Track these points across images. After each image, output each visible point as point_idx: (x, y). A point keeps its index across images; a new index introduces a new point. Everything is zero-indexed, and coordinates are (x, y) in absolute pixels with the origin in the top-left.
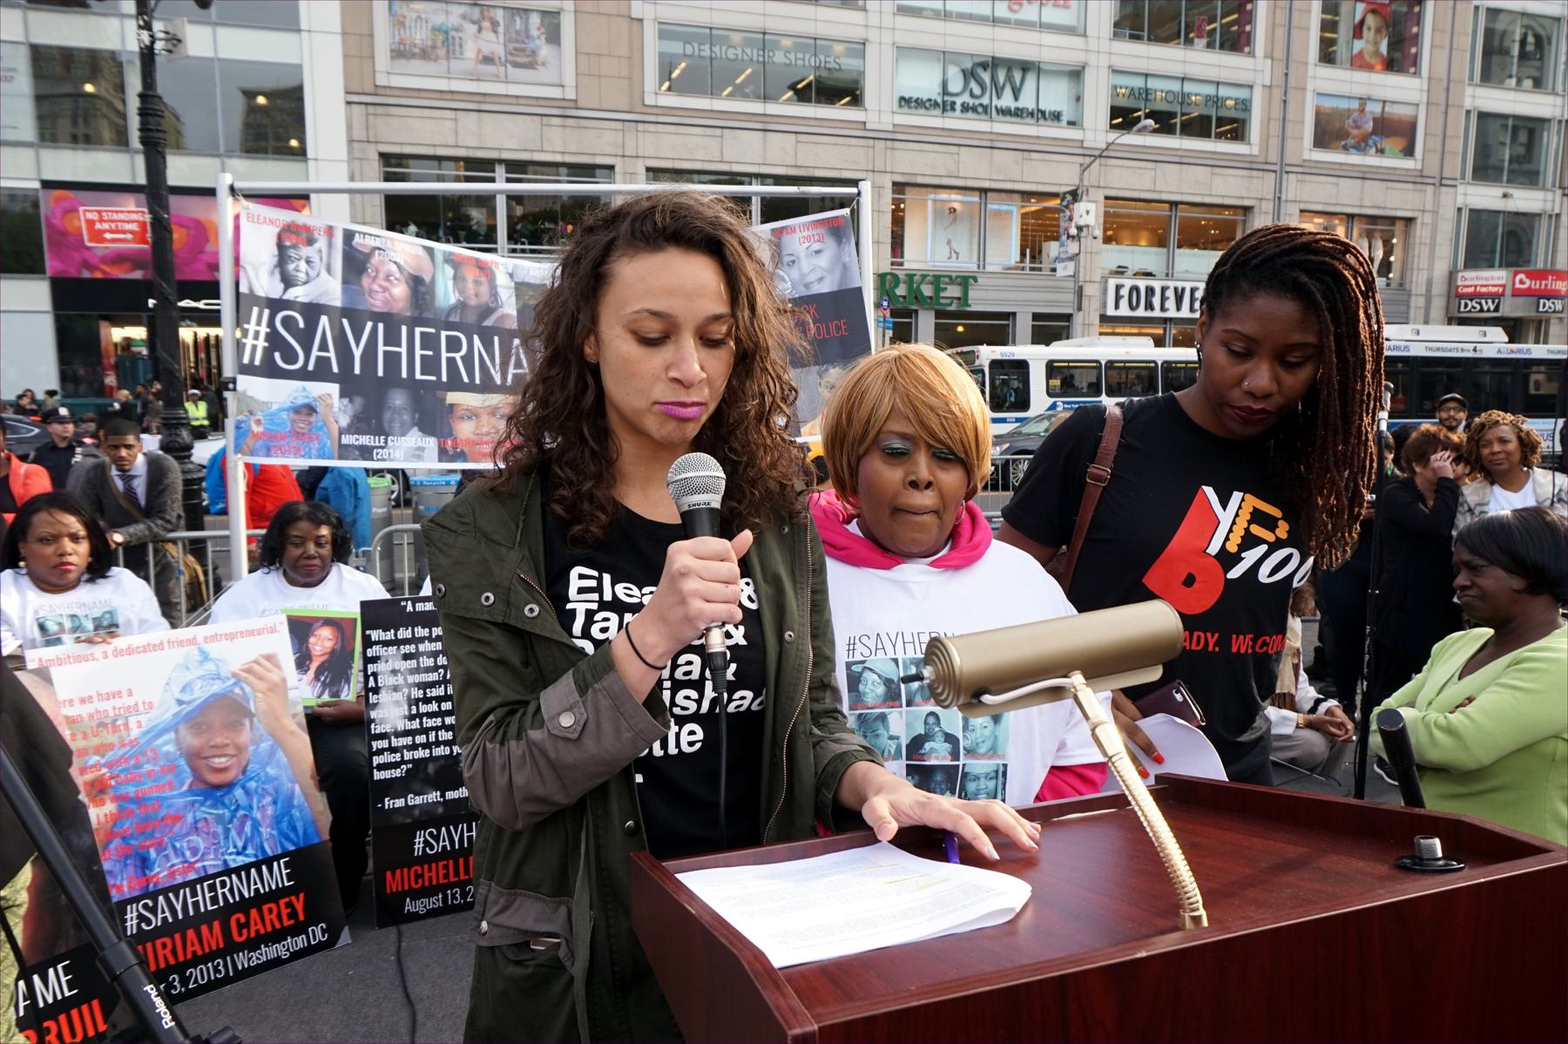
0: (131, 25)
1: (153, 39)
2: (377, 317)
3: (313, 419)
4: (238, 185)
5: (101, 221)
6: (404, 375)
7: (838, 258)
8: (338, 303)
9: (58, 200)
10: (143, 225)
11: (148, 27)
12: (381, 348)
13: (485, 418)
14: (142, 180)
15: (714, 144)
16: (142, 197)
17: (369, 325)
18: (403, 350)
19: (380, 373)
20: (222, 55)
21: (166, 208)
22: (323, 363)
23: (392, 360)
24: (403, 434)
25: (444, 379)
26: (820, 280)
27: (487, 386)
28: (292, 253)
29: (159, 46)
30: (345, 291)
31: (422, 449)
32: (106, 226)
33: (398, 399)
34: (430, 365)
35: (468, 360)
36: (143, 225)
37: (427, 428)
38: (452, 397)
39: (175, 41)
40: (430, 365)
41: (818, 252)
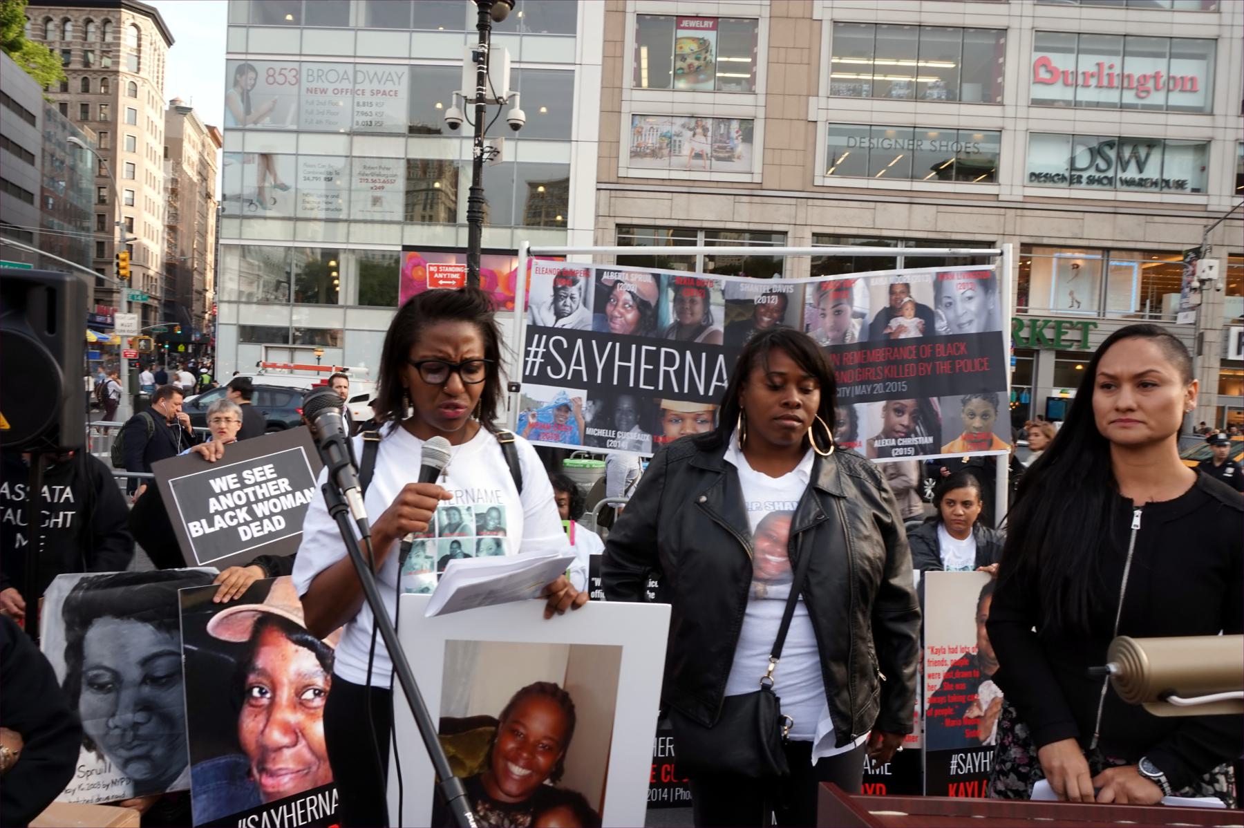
0: (472, 142)
1: (483, 152)
2: (614, 338)
3: (568, 415)
4: (533, 249)
5: (438, 272)
6: (631, 384)
7: (984, 305)
8: (590, 328)
9: (411, 258)
10: (462, 274)
11: (480, 144)
12: (617, 363)
13: (689, 422)
14: (464, 243)
15: (868, 215)
16: (464, 256)
17: (610, 344)
18: (632, 365)
20: (519, 160)
21: (477, 263)
22: (577, 374)
25: (661, 388)
26: (970, 322)
27: (693, 396)
28: (562, 293)
29: (485, 156)
31: (640, 442)
32: (441, 276)
35: (680, 373)
36: (462, 274)
38: (666, 404)
39: (495, 152)
41: (970, 298)
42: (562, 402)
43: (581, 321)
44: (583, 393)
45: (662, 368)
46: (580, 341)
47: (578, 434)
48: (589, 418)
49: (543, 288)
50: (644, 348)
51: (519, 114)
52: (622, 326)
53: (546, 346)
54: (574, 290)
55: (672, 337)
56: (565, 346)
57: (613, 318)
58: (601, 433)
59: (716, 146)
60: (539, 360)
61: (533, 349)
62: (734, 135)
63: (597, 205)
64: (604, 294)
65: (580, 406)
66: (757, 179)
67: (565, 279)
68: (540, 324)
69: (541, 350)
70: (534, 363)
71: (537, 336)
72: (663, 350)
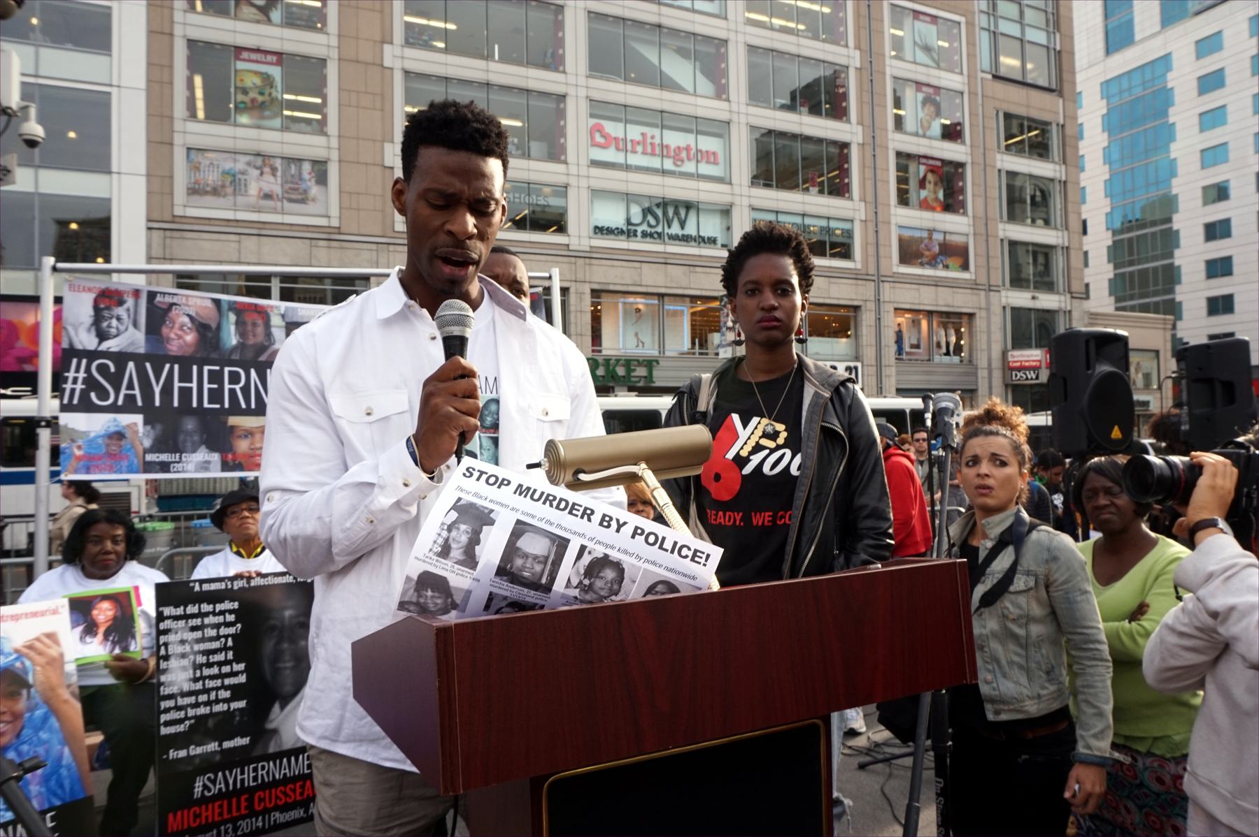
2: (174, 360)
6: (195, 404)
8: (142, 351)
12: (177, 384)
17: (167, 366)
18: (194, 385)
19: (176, 404)
20: (42, 190)
23: (186, 393)
24: (194, 451)
28: (106, 314)
30: (147, 340)
31: (208, 462)
33: (190, 424)
34: (216, 396)
37: (212, 448)
40: (216, 396)
42: (113, 429)
43: (132, 344)
44: (138, 419)
45: (227, 386)
46: (131, 365)
47: (136, 462)
48: (147, 443)
49: (81, 308)
50: (206, 368)
51: (35, 129)
52: (180, 347)
53: (88, 370)
54: (121, 311)
55: (236, 357)
56: (113, 369)
57: (169, 340)
58: (164, 457)
59: (287, 186)
60: (79, 386)
61: (71, 375)
62: (306, 176)
63: (149, 246)
64: (157, 316)
65: (137, 432)
66: (335, 223)
67: (107, 300)
68: (79, 347)
69: (82, 375)
70: (73, 391)
71: (75, 361)
72: (227, 369)
